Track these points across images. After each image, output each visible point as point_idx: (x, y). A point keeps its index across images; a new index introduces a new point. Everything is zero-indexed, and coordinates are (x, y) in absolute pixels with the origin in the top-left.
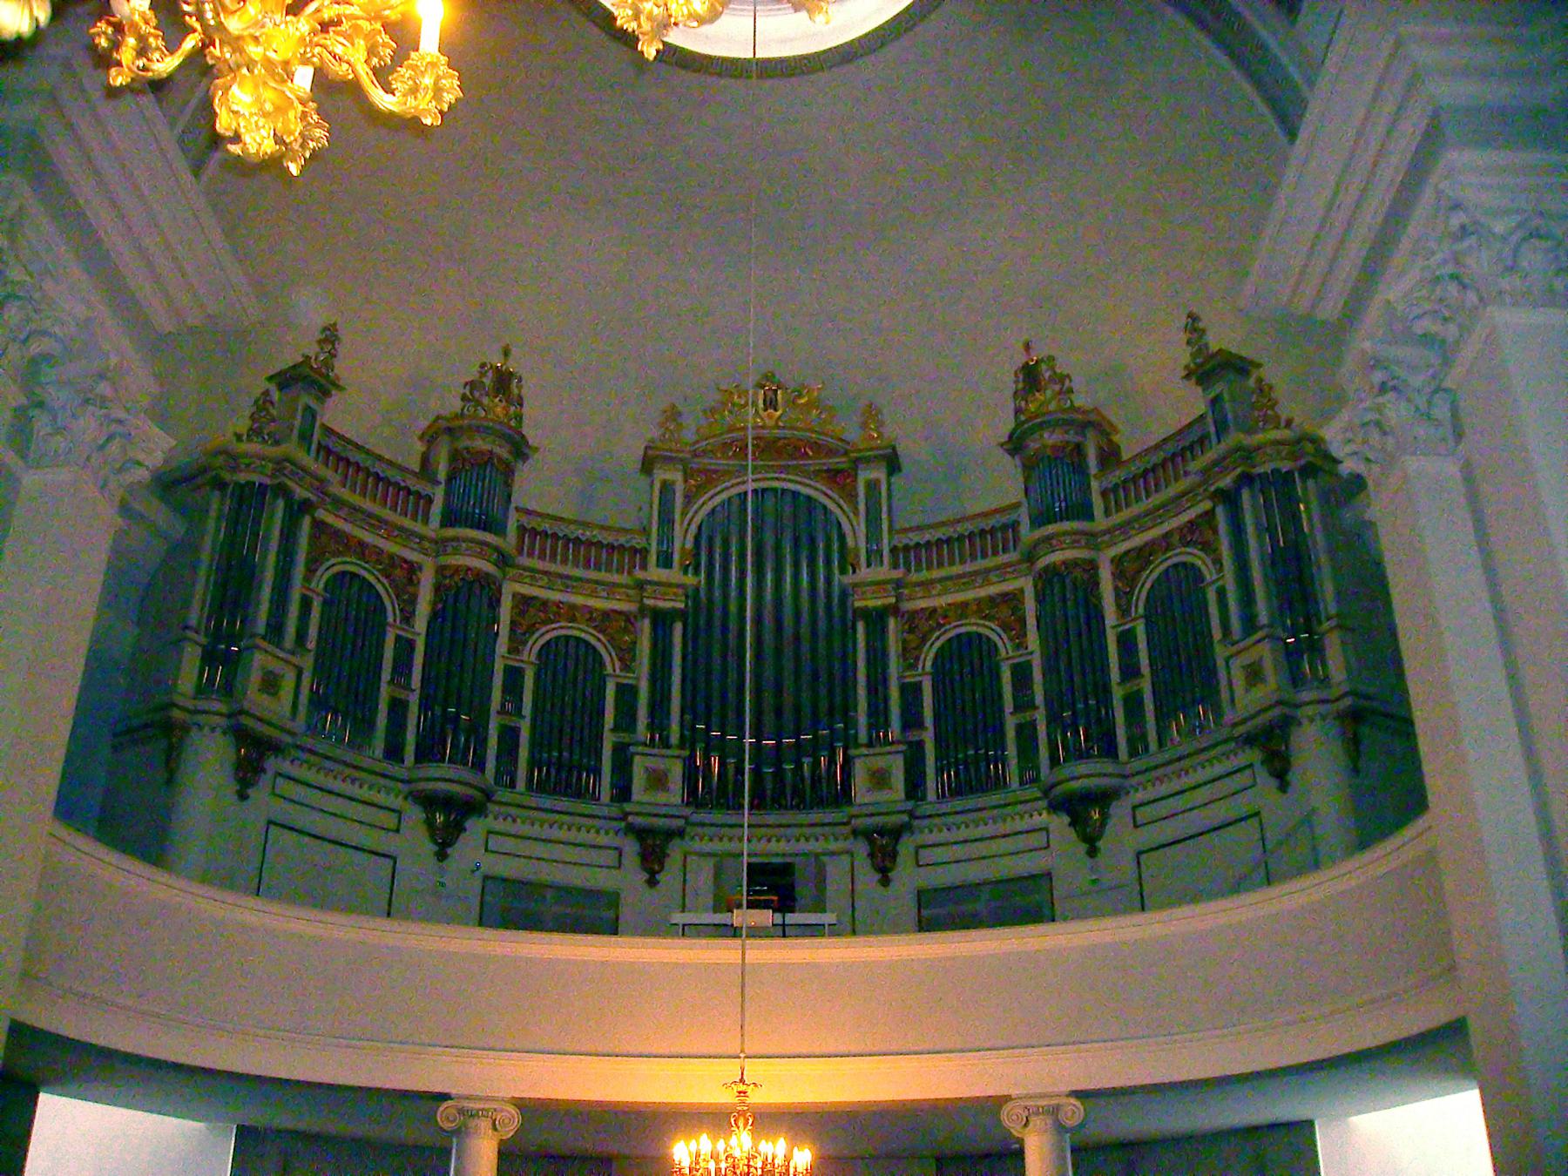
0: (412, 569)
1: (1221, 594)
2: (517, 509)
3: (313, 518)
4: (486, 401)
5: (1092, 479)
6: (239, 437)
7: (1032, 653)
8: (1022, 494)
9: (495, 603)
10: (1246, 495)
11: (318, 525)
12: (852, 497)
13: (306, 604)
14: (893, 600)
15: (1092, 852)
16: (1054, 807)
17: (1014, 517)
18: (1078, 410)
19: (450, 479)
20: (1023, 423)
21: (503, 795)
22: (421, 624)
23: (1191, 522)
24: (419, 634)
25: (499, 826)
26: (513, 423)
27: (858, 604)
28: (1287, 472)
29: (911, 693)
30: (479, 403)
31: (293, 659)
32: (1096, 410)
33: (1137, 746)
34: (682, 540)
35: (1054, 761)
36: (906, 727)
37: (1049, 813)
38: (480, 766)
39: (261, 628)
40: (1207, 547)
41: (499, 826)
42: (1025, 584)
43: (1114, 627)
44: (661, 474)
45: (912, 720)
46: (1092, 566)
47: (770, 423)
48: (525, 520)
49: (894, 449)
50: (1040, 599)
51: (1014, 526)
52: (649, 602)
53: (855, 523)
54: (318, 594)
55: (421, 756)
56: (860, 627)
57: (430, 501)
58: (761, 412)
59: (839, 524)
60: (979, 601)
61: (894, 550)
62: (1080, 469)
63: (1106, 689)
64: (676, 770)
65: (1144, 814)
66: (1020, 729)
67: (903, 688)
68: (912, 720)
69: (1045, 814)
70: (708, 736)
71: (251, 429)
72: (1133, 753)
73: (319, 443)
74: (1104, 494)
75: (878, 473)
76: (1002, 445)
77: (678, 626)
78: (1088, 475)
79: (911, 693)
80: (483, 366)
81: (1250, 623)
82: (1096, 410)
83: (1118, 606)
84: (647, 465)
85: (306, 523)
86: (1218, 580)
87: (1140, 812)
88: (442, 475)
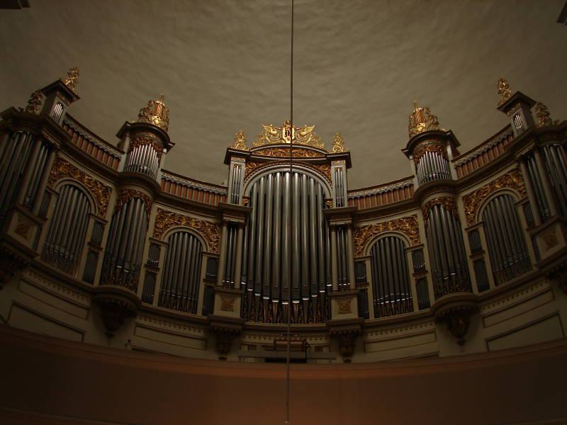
0: (106, 191)
1: (526, 205)
2: (162, 170)
3: (57, 155)
4: (149, 116)
5: (450, 163)
6: (22, 110)
7: (423, 245)
8: (414, 173)
9: (148, 211)
10: (536, 156)
11: (58, 159)
12: (328, 176)
13: (49, 194)
14: (350, 222)
15: (461, 343)
16: (439, 321)
17: (409, 182)
18: (442, 131)
19: (129, 152)
20: (414, 138)
21: (144, 304)
22: (108, 217)
23: (505, 175)
24: (107, 222)
25: (142, 321)
26: (163, 128)
27: (331, 223)
28: (557, 146)
29: (359, 264)
30: (148, 118)
31: (39, 220)
32: (450, 131)
33: (483, 286)
34: (243, 192)
35: (437, 295)
36: (356, 281)
37: (436, 323)
38: (135, 288)
39: (21, 202)
40: (514, 185)
41: (142, 321)
42: (419, 213)
43: (466, 229)
44: (234, 161)
45: (361, 282)
46: (454, 203)
47: (289, 142)
48: (165, 175)
49: (349, 153)
50: (426, 217)
51: (411, 185)
52: (225, 218)
53: (330, 189)
54: (55, 192)
55: (102, 280)
56: (333, 233)
57: (119, 159)
58: (284, 137)
59: (322, 188)
60: (393, 222)
61: (349, 199)
62: (445, 157)
63: (466, 262)
64: (238, 302)
65: (488, 321)
66: (418, 282)
67: (356, 264)
68: (361, 282)
69: (433, 323)
70: (254, 288)
71: (27, 107)
72: (480, 291)
73: (64, 122)
74: (457, 168)
75: (341, 164)
76: (403, 150)
77: (241, 231)
78: (448, 161)
79: (359, 264)
80: (150, 102)
81: (543, 219)
82: (450, 131)
83: (468, 219)
84: (227, 161)
85: (54, 154)
86: (524, 199)
87: (486, 320)
88: (126, 149)
